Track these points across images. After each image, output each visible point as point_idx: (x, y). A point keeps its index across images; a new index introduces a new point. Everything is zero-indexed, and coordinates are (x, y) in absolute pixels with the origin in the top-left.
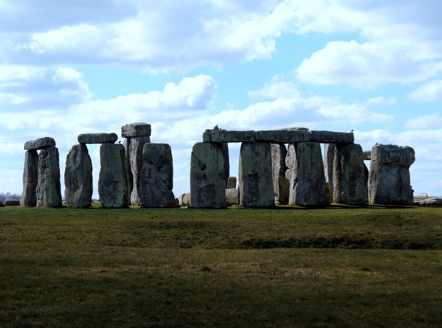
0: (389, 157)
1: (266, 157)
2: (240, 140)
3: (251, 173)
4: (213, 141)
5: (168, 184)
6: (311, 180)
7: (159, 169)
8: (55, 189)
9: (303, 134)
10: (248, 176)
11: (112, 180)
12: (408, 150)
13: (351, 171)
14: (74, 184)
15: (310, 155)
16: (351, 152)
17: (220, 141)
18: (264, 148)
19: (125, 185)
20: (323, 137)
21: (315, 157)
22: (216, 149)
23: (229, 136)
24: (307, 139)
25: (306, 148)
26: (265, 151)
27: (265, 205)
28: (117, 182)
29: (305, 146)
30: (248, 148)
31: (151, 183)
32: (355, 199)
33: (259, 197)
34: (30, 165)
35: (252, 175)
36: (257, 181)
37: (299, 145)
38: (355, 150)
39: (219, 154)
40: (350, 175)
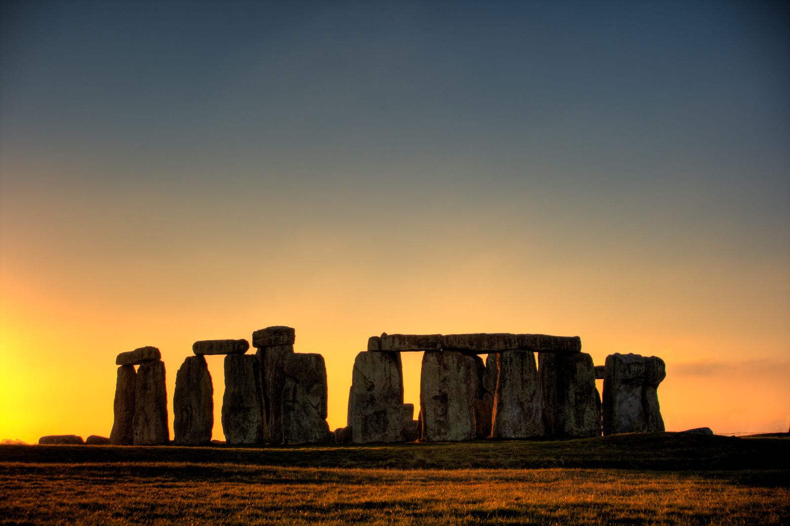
1: (458, 371)
3: (438, 394)
4: (383, 349)
5: (320, 411)
6: (521, 403)
8: (160, 420)
11: (241, 405)
13: (577, 391)
14: (187, 411)
17: (395, 350)
18: (455, 359)
19: (260, 413)
20: (538, 344)
21: (528, 371)
22: (388, 361)
23: (407, 343)
26: (458, 363)
27: (459, 439)
28: (248, 409)
29: (512, 356)
30: (433, 358)
31: (296, 409)
32: (584, 430)
33: (449, 428)
34: (124, 387)
35: (439, 396)
36: (447, 406)
38: (582, 360)
39: (393, 367)
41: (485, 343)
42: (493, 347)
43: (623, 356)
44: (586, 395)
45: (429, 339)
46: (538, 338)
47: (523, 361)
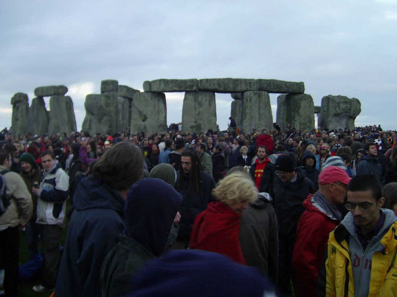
0: (339, 108)
1: (210, 107)
2: (181, 89)
3: (194, 124)
7: (100, 120)
9: (250, 83)
10: (190, 127)
12: (355, 102)
13: (301, 122)
15: (257, 104)
16: (301, 102)
17: (160, 90)
18: (208, 98)
20: (272, 87)
24: (255, 87)
25: (253, 98)
30: (191, 97)
35: (194, 126)
37: (246, 94)
38: (305, 100)
40: (300, 127)
41: (231, 86)
42: (236, 88)
43: (334, 97)
44: (308, 125)
45: (187, 82)
46: (272, 82)
47: (260, 100)
